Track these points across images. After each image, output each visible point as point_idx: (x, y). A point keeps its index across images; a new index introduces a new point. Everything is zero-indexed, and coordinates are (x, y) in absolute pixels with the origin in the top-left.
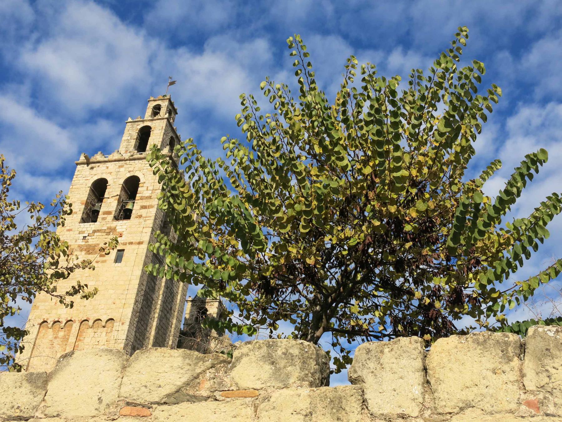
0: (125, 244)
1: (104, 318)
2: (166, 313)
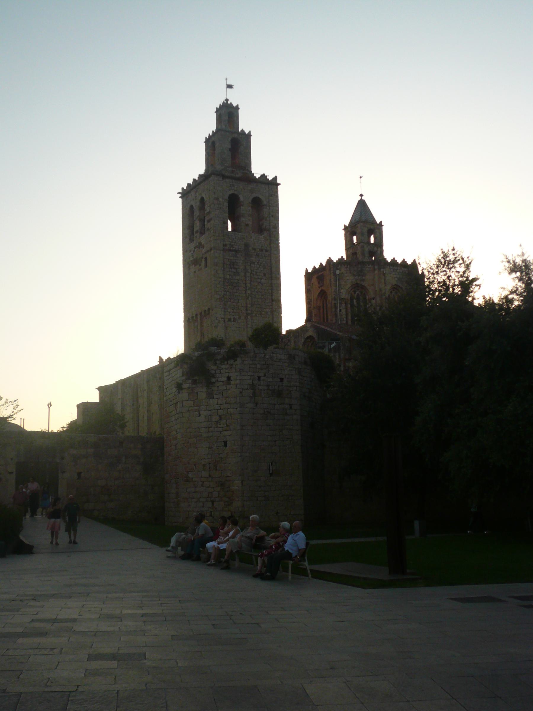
0: (206, 253)
1: (206, 309)
2: (259, 281)
